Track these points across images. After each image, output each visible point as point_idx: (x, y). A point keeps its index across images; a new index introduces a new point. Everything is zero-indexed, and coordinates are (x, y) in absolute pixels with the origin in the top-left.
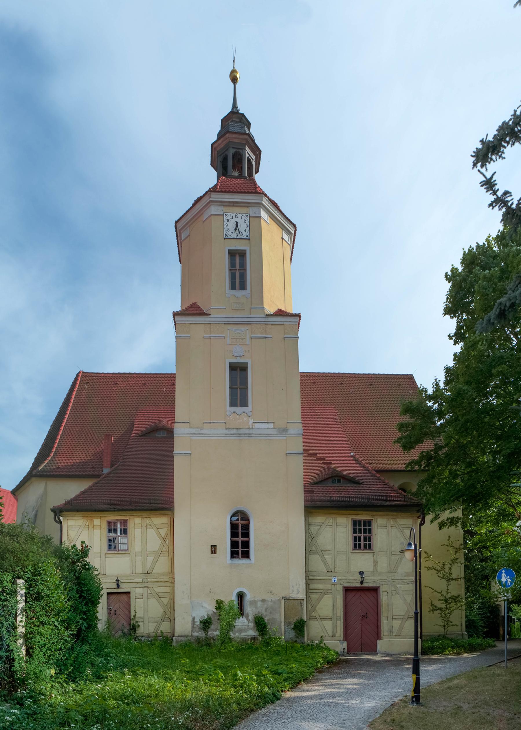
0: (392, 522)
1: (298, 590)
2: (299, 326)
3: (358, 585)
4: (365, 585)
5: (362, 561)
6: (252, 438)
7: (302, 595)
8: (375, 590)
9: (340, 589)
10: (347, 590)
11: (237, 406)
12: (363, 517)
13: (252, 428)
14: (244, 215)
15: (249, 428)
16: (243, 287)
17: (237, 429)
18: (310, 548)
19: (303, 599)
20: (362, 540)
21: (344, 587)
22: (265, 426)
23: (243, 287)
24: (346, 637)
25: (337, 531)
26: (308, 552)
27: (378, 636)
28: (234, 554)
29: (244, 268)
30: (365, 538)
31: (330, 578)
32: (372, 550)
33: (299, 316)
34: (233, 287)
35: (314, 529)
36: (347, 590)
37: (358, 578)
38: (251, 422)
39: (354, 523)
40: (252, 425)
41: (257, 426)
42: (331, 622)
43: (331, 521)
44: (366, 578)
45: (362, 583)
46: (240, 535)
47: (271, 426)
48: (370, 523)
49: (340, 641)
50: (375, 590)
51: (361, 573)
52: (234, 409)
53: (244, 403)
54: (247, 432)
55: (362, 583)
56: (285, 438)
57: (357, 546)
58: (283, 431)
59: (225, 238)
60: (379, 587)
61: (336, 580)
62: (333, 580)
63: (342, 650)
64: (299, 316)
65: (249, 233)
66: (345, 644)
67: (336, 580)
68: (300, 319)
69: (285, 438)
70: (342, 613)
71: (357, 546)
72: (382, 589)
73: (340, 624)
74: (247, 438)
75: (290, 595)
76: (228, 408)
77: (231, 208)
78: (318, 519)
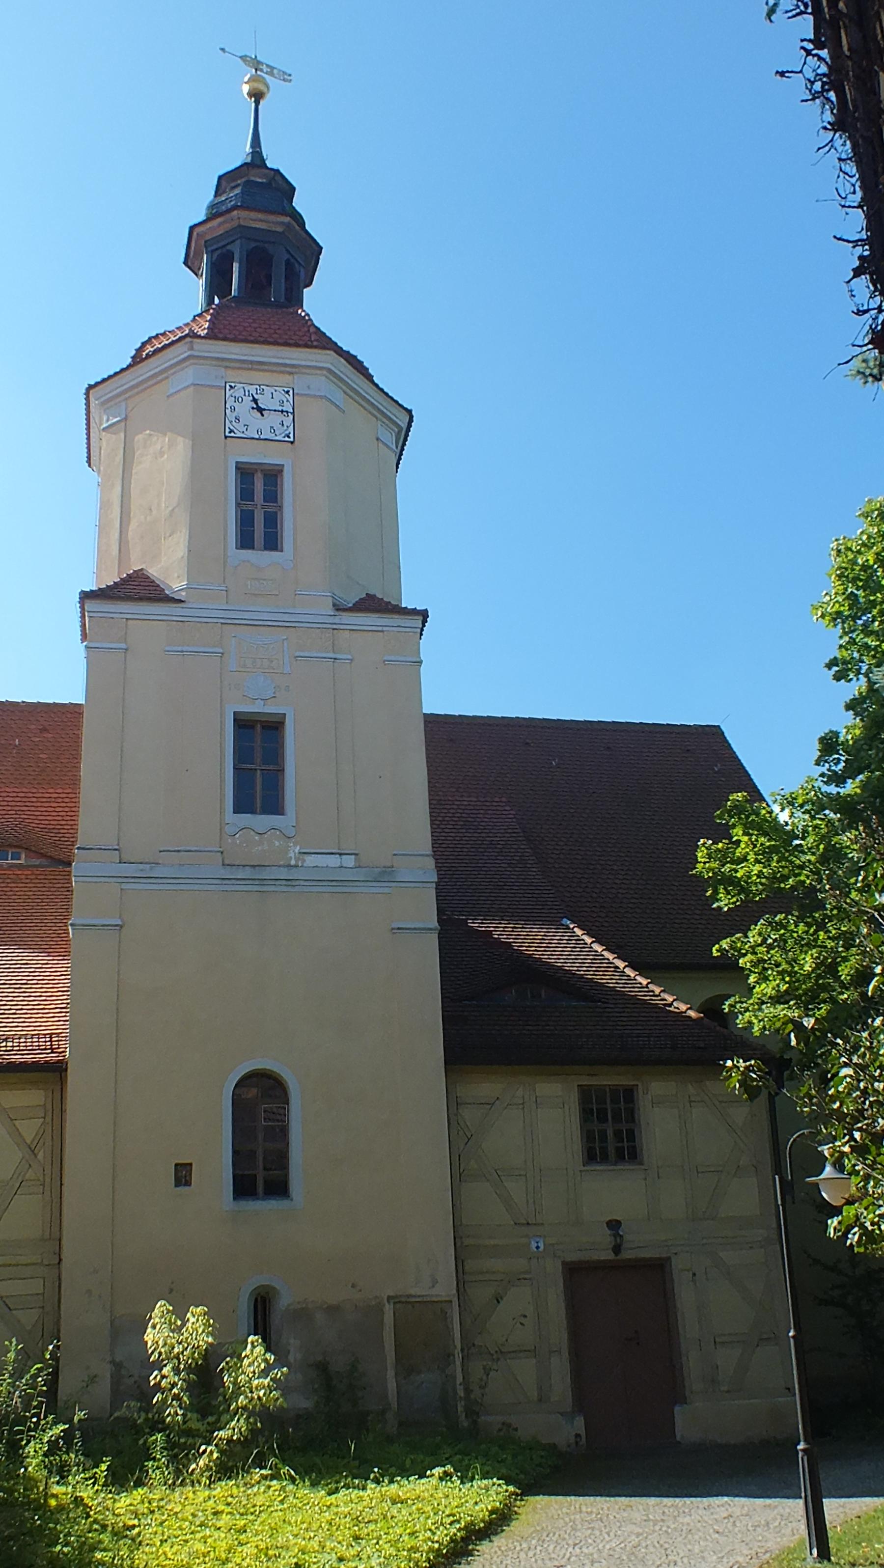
0: (691, 1089)
1: (430, 1273)
2: (421, 634)
3: (609, 1256)
4: (626, 1255)
5: (614, 1193)
6: (296, 889)
7: (444, 1288)
8: (657, 1269)
9: (554, 1268)
10: (575, 1272)
11: (253, 812)
12: (610, 1079)
13: (296, 866)
14: (280, 389)
15: (289, 866)
16: (273, 543)
17: (254, 866)
18: (464, 1161)
19: (451, 1302)
20: (610, 1135)
21: (564, 1264)
22: (333, 861)
23: (273, 543)
24: (582, 1401)
25: (540, 1116)
26: (459, 1176)
27: (676, 1394)
28: (244, 1188)
29: (276, 502)
30: (618, 1134)
31: (524, 1240)
32: (641, 1164)
33: (424, 615)
34: (245, 541)
35: (468, 1114)
36: (575, 1272)
37: (605, 1237)
38: (294, 851)
39: (585, 1093)
40: (297, 860)
41: (310, 860)
42: (534, 1361)
43: (520, 1093)
44: (627, 1237)
45: (617, 1249)
46: (261, 1137)
47: (349, 861)
48: (629, 1094)
49: (562, 1414)
50: (657, 1269)
51: (614, 1225)
52: (246, 819)
53: (274, 805)
54: (283, 874)
55: (617, 1249)
56: (386, 890)
57: (595, 1154)
58: (385, 875)
59: (226, 437)
60: (669, 1258)
61: (541, 1245)
62: (534, 1245)
63: (572, 1440)
64: (424, 615)
65: (291, 429)
66: (580, 1423)
67: (541, 1245)
68: (424, 622)
69: (386, 890)
70: (565, 1336)
71: (595, 1154)
72: (677, 1264)
73: (560, 1368)
74: (285, 889)
75: (412, 1292)
76: (230, 816)
77: (245, 373)
78: (485, 1087)
